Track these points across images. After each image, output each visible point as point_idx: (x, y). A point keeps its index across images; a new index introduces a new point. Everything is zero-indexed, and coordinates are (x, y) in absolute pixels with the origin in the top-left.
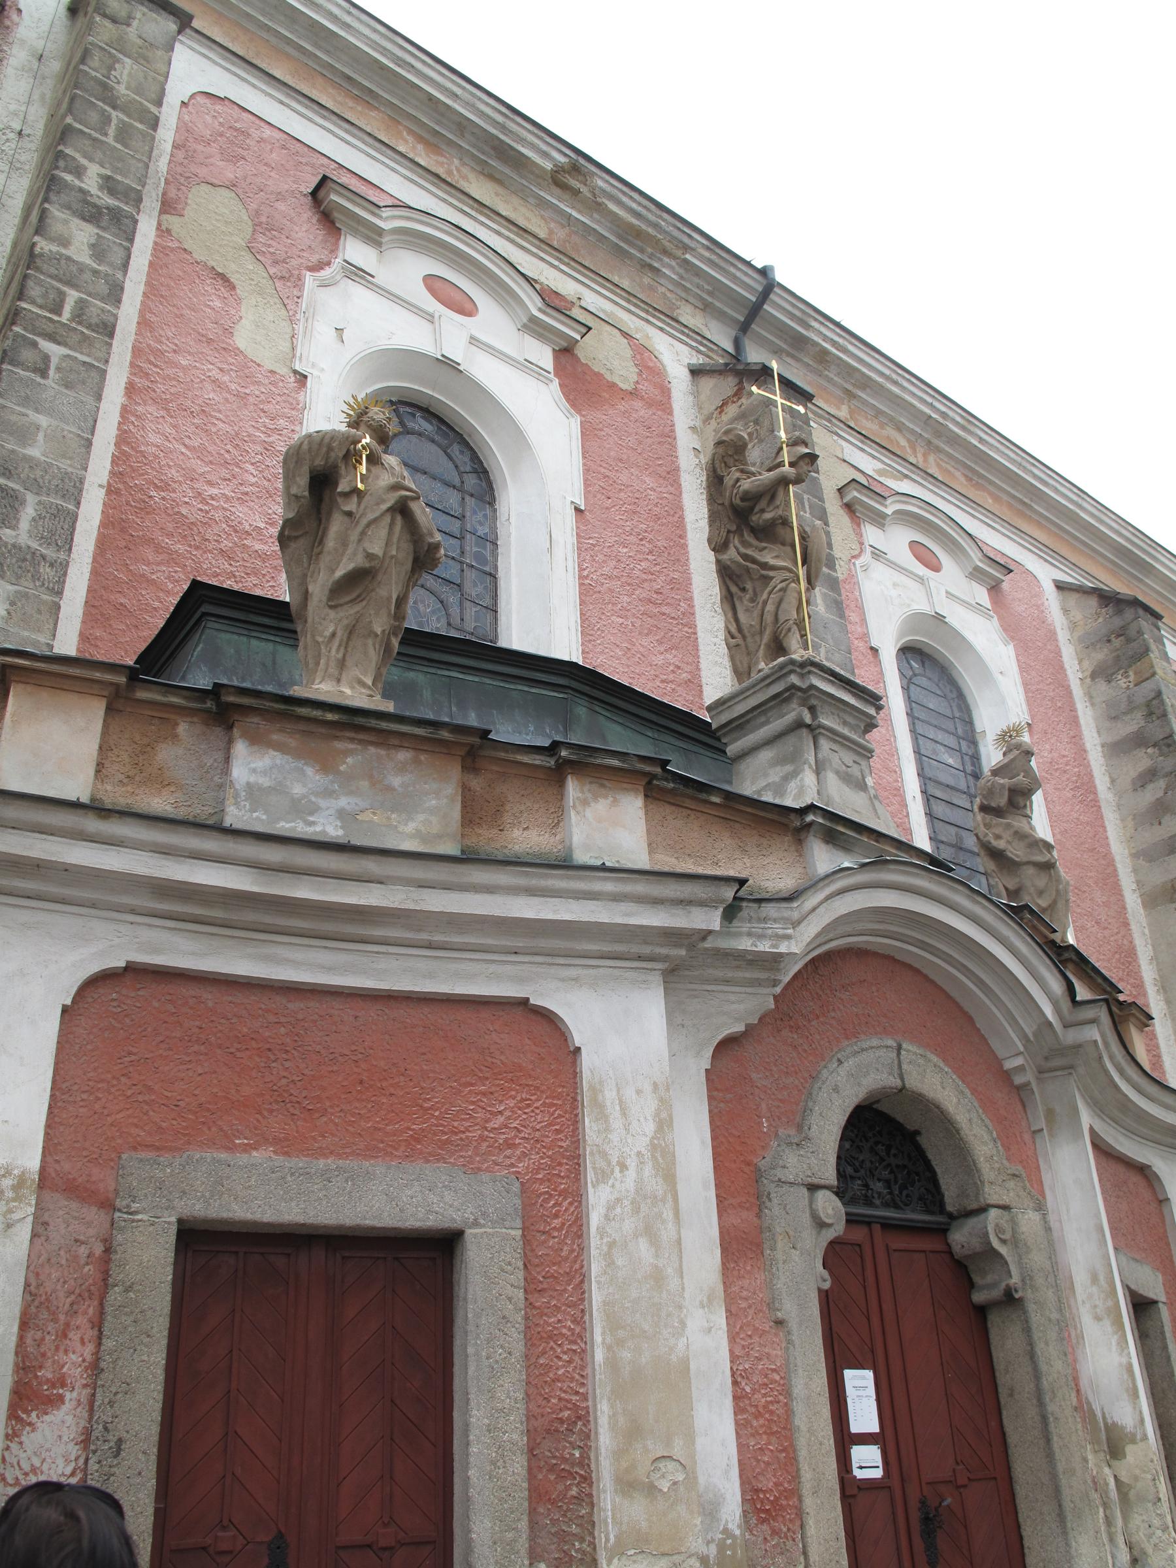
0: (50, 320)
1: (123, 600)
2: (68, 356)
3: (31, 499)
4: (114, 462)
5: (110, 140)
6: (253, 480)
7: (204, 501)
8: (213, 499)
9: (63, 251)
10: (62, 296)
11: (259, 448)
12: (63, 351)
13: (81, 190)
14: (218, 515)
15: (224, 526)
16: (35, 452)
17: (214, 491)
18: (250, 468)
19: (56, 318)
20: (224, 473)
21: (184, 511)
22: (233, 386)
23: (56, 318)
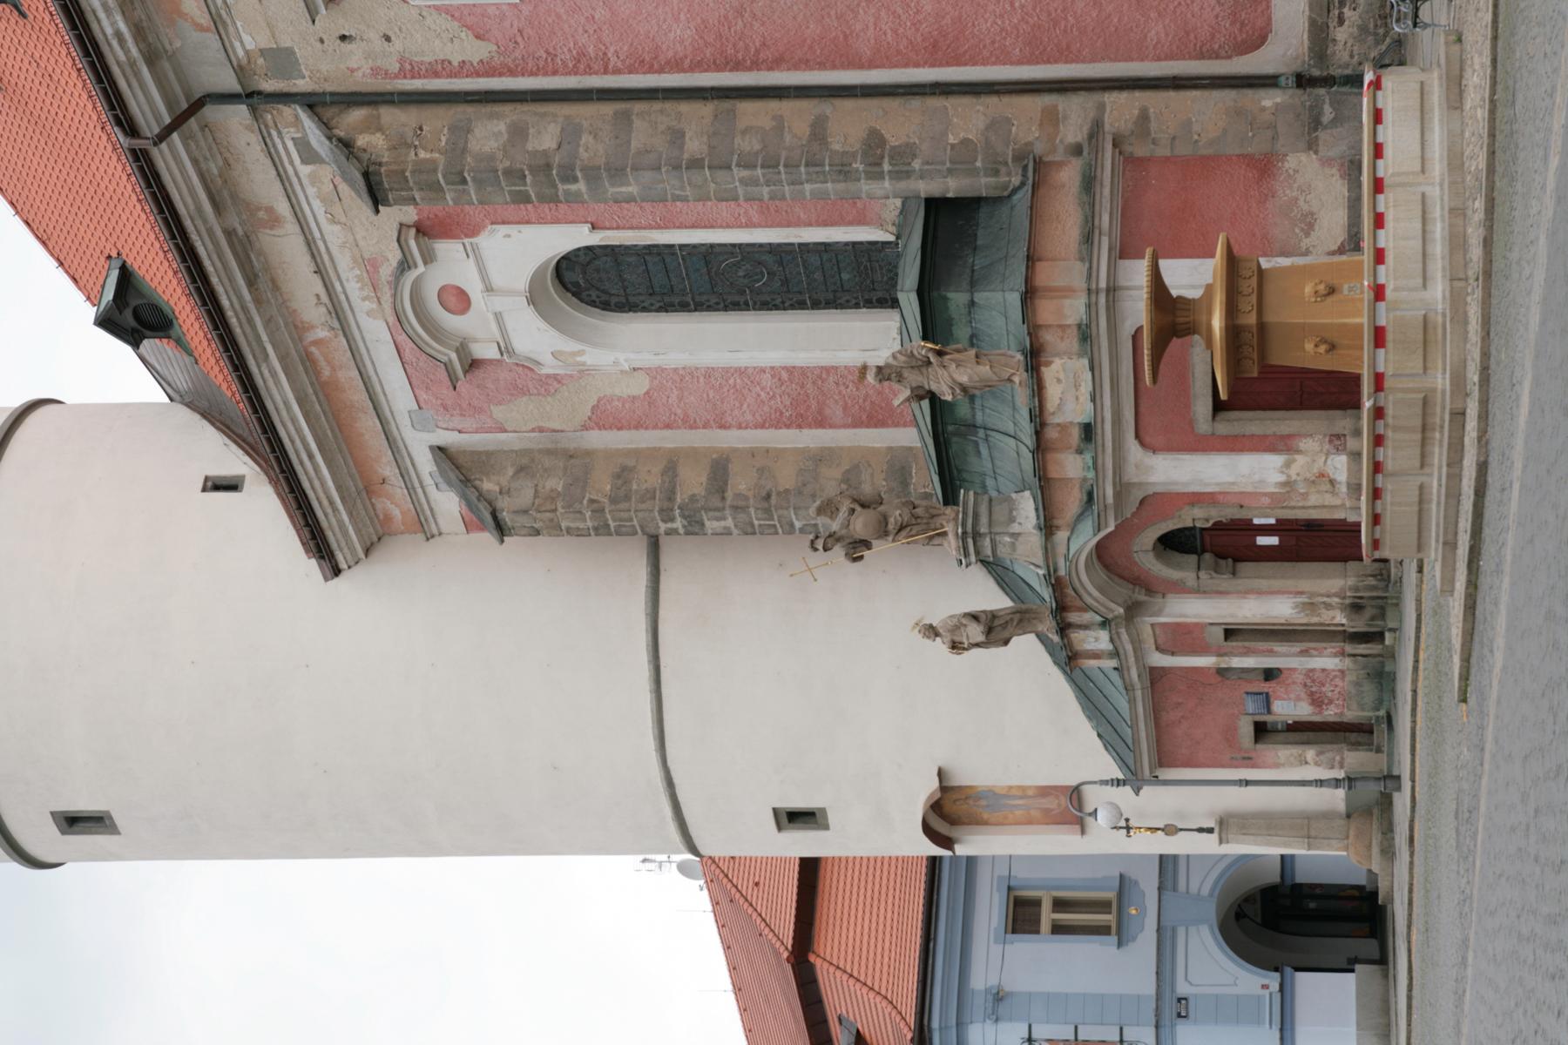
0: (781, 526)
1: (864, 417)
2: (797, 519)
4: (781, 428)
5: (635, 522)
6: (738, 381)
7: (774, 396)
8: (768, 393)
9: (733, 527)
10: (760, 525)
13: (684, 526)
14: (778, 391)
15: (783, 388)
18: (731, 381)
19: (778, 526)
20: (745, 391)
21: (788, 403)
22: (676, 393)
23: (778, 526)
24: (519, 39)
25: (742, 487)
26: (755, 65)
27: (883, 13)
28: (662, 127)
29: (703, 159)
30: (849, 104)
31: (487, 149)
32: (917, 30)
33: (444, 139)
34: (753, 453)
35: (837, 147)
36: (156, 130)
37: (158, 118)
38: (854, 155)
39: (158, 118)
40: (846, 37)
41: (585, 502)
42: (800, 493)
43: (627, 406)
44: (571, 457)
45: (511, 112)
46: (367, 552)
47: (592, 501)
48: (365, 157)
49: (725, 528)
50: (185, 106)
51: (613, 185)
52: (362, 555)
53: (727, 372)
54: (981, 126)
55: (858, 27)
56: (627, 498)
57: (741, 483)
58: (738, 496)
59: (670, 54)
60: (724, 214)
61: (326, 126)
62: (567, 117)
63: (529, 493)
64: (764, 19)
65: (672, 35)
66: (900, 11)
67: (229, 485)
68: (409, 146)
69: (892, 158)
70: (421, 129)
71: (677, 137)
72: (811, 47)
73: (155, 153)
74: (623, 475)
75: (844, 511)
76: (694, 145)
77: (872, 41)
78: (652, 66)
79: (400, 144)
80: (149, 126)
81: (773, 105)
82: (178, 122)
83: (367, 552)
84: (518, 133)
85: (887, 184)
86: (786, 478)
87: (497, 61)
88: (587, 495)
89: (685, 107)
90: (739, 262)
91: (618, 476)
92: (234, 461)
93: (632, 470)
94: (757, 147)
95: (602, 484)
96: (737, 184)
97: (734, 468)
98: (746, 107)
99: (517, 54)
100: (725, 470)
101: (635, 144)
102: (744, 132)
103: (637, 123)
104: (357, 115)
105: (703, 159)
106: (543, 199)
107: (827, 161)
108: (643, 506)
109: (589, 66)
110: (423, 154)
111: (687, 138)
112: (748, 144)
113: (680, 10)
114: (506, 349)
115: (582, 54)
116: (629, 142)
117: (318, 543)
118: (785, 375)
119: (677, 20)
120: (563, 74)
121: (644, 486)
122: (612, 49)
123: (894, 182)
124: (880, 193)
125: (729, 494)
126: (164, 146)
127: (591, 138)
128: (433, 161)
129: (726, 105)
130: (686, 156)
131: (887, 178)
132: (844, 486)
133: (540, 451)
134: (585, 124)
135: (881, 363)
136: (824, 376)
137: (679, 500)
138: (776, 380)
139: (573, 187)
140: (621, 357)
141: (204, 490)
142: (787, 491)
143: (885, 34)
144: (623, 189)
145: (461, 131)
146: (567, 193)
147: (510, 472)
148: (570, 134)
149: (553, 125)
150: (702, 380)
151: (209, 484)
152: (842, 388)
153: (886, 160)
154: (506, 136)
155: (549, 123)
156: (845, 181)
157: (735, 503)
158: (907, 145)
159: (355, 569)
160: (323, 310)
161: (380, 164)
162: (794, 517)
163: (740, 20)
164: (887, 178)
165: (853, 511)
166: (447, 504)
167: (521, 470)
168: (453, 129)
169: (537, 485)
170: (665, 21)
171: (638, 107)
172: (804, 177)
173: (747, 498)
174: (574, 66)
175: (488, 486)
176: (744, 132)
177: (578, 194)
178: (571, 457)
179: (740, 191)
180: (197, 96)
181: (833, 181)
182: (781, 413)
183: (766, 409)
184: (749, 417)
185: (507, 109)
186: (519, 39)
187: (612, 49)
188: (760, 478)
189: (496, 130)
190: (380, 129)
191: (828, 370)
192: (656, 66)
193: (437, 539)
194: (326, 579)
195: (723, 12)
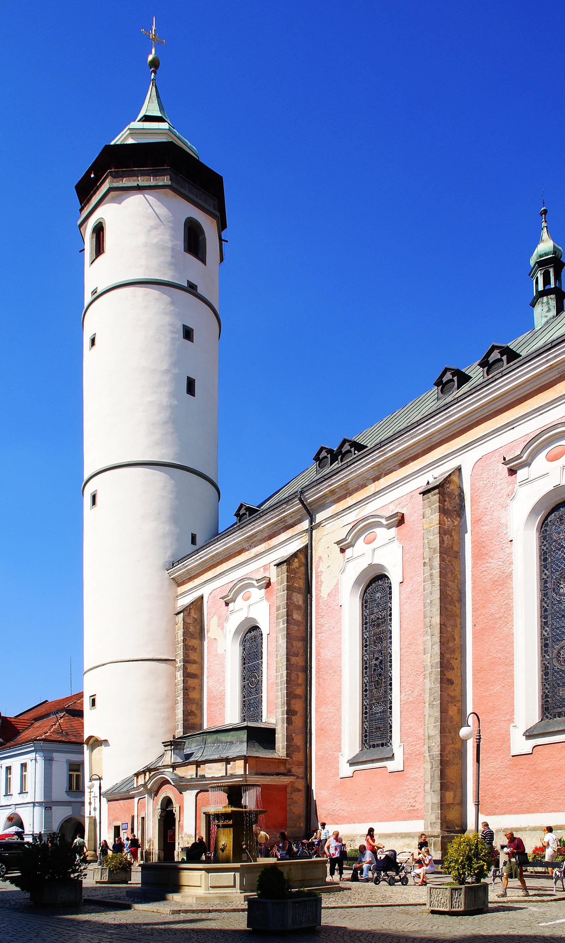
3: (179, 723)
6: (221, 680)
10: (178, 688)
11: (222, 673)
12: (179, 698)
16: (179, 717)
17: (217, 688)
18: (221, 678)
24: (327, 607)
26: (318, 678)
27: (333, 714)
28: (299, 650)
32: (327, 724)
33: (297, 585)
40: (326, 703)
43: (214, 649)
49: (178, 678)
51: (281, 636)
53: (224, 677)
54: (298, 744)
55: (329, 707)
59: (322, 652)
60: (271, 672)
64: (332, 679)
65: (328, 652)
66: (334, 719)
70: (300, 579)
72: (323, 693)
77: (324, 711)
78: (318, 647)
85: (281, 716)
87: (321, 601)
90: (257, 678)
93: (195, 651)
94: (292, 678)
96: (281, 672)
99: (323, 607)
100: (195, 678)
106: (278, 615)
109: (319, 628)
111: (296, 658)
113: (336, 654)
114: (232, 612)
115: (322, 626)
118: (223, 693)
119: (332, 653)
120: (316, 621)
122: (324, 635)
123: (281, 719)
124: (277, 715)
125: (187, 678)
131: (282, 716)
132: (189, 711)
136: (222, 704)
138: (221, 691)
139: (281, 624)
143: (327, 715)
144: (280, 639)
146: (280, 622)
148: (297, 623)
149: (301, 618)
150: (222, 670)
152: (219, 710)
154: (297, 604)
156: (281, 704)
157: (185, 680)
158: (292, 722)
162: (180, 697)
163: (332, 672)
164: (282, 716)
168: (300, 588)
170: (332, 650)
172: (283, 692)
173: (186, 683)
174: (319, 624)
177: (279, 625)
179: (279, 674)
181: (281, 701)
182: (212, 693)
183: (213, 689)
184: (211, 684)
186: (327, 607)
187: (324, 635)
188: (192, 688)
189: (300, 601)
191: (224, 705)
192: (318, 648)
195: (335, 667)
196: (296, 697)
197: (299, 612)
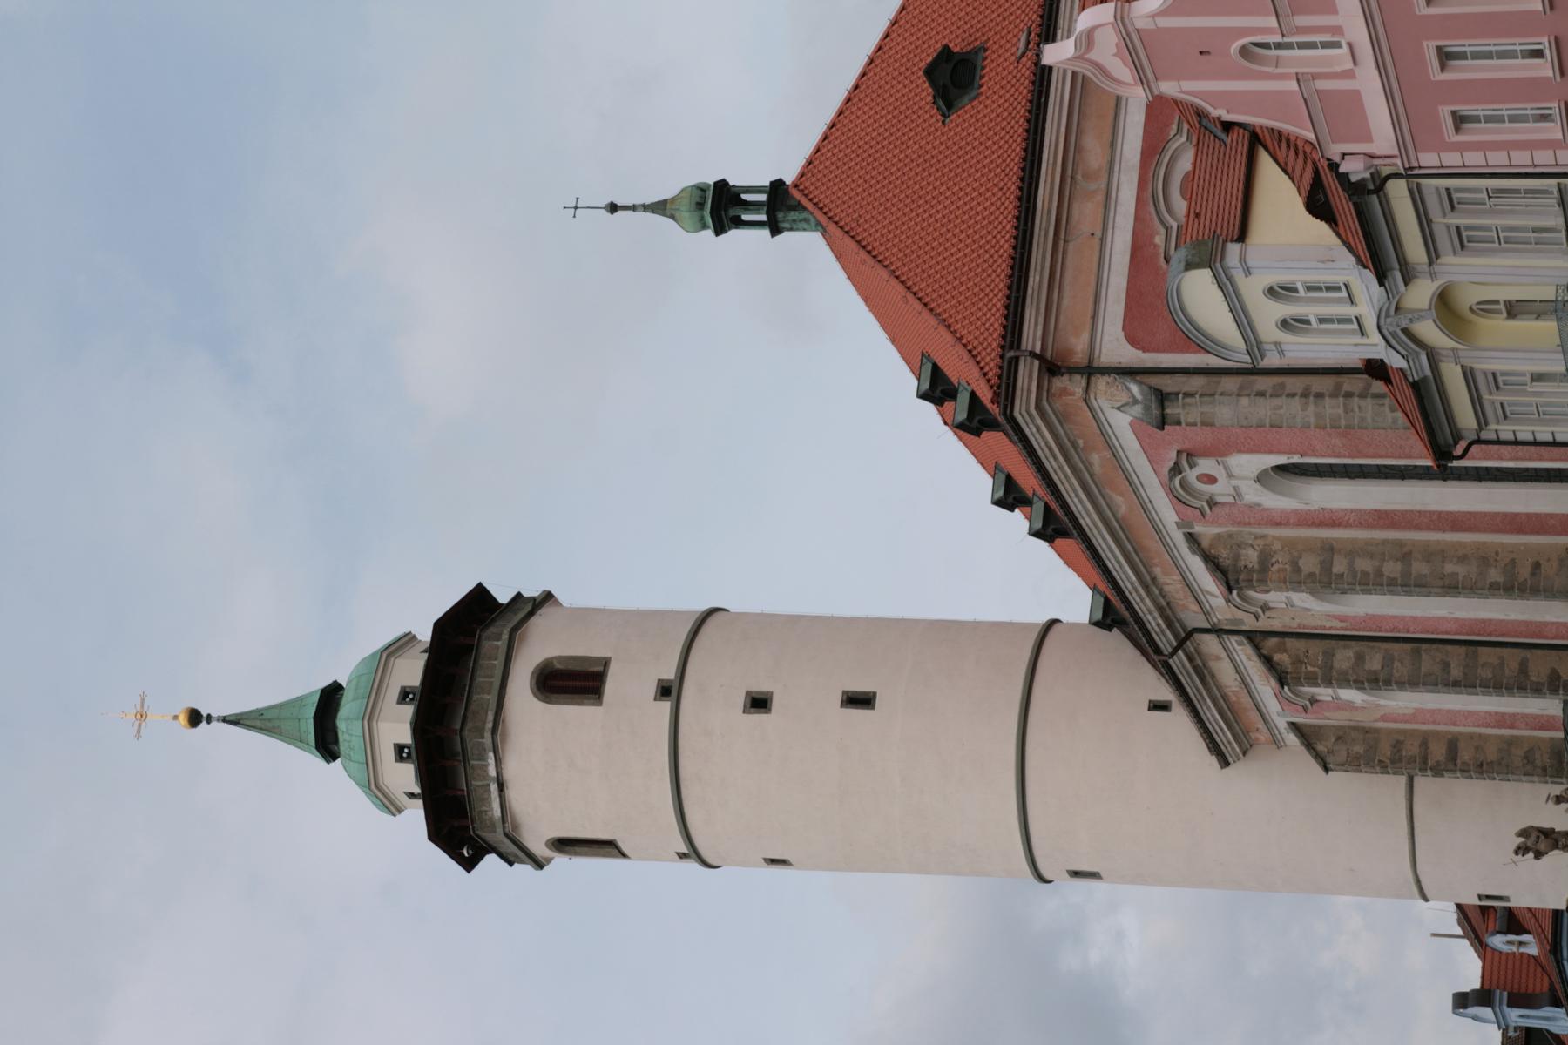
25: (1466, 758)
28: (1438, 660)
29: (1460, 681)
30: (1539, 652)
31: (1343, 667)
33: (1320, 659)
34: (1471, 736)
35: (1533, 679)
36: (1170, 650)
37: (1170, 644)
38: (1543, 684)
39: (1170, 644)
41: (1376, 762)
42: (1500, 764)
44: (1367, 732)
45: (1356, 647)
46: (1244, 753)
47: (1380, 761)
48: (1279, 668)
50: (1183, 635)
52: (1241, 755)
56: (1400, 760)
57: (1465, 755)
58: (1464, 763)
61: (1257, 648)
62: (1386, 650)
63: (1344, 753)
67: (1159, 706)
68: (1301, 662)
69: (1564, 687)
70: (1307, 652)
71: (1446, 666)
73: (1171, 661)
74: (1397, 745)
75: (1533, 838)
76: (1456, 672)
79: (1297, 662)
80: (1167, 650)
81: (1498, 650)
82: (1181, 644)
83: (1244, 753)
84: (1360, 658)
86: (1491, 754)
88: (1377, 758)
89: (1449, 648)
91: (1394, 747)
92: (1166, 693)
94: (1490, 675)
95: (1386, 751)
97: (1461, 745)
98: (1481, 649)
101: (1423, 669)
102: (1484, 665)
103: (1424, 656)
104: (1273, 641)
105: (1460, 681)
107: (1529, 687)
108: (1409, 766)
110: (1309, 668)
112: (1486, 673)
116: (1420, 668)
117: (1225, 763)
121: (1410, 754)
125: (1459, 762)
126: (1175, 657)
127: (1399, 665)
128: (1315, 673)
129: (1473, 648)
130: (1451, 679)
133: (1349, 727)
134: (1396, 654)
135: (1558, 794)
137: (1430, 764)
140: (1400, 703)
141: (1149, 709)
142: (1492, 762)
145: (1329, 655)
147: (1333, 740)
148: (1388, 661)
151: (1152, 704)
153: (1561, 689)
154: (1353, 660)
155: (1376, 653)
157: (1462, 768)
159: (1238, 763)
160: (1237, 683)
161: (1287, 673)
165: (1538, 837)
166: (1292, 739)
167: (1339, 738)
168: (1325, 653)
169: (1348, 749)
171: (1424, 646)
173: (1468, 765)
175: (1320, 748)
176: (1484, 665)
178: (1367, 732)
180: (1189, 629)
185: (1353, 643)
189: (1348, 655)
190: (1285, 651)
193: (1284, 749)
194: (1222, 768)
196: (1524, 669)
197: (1367, 657)
